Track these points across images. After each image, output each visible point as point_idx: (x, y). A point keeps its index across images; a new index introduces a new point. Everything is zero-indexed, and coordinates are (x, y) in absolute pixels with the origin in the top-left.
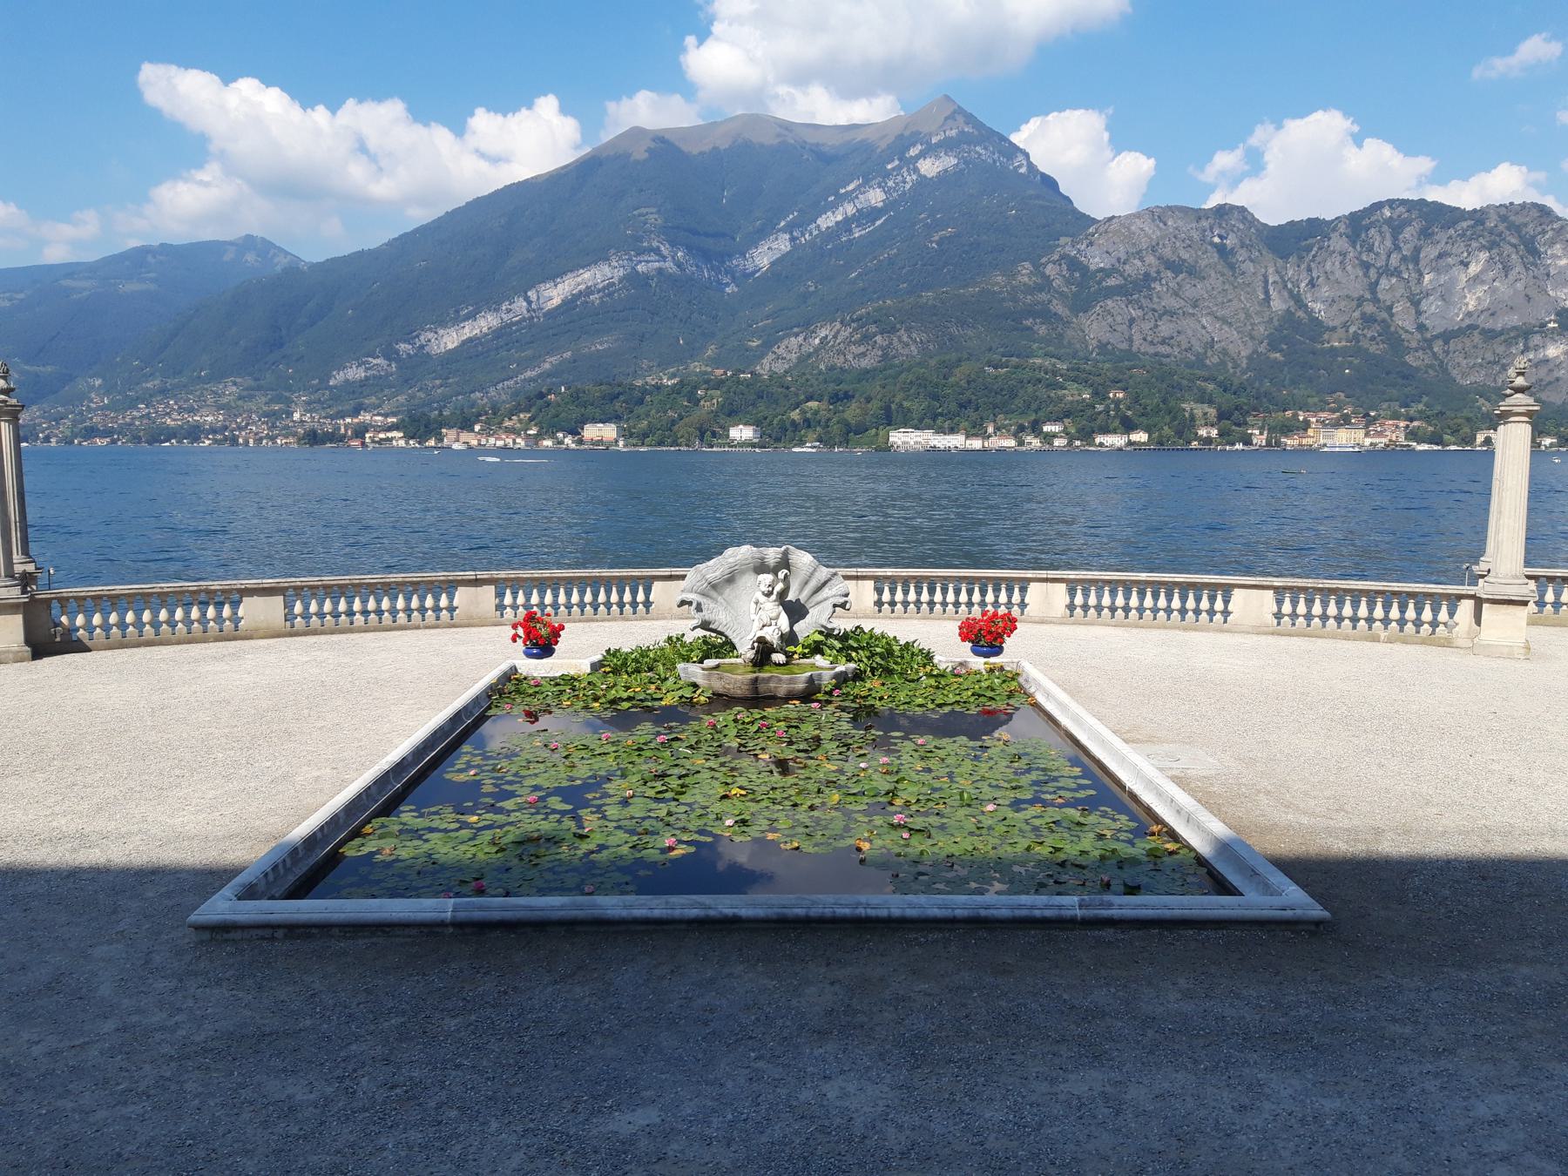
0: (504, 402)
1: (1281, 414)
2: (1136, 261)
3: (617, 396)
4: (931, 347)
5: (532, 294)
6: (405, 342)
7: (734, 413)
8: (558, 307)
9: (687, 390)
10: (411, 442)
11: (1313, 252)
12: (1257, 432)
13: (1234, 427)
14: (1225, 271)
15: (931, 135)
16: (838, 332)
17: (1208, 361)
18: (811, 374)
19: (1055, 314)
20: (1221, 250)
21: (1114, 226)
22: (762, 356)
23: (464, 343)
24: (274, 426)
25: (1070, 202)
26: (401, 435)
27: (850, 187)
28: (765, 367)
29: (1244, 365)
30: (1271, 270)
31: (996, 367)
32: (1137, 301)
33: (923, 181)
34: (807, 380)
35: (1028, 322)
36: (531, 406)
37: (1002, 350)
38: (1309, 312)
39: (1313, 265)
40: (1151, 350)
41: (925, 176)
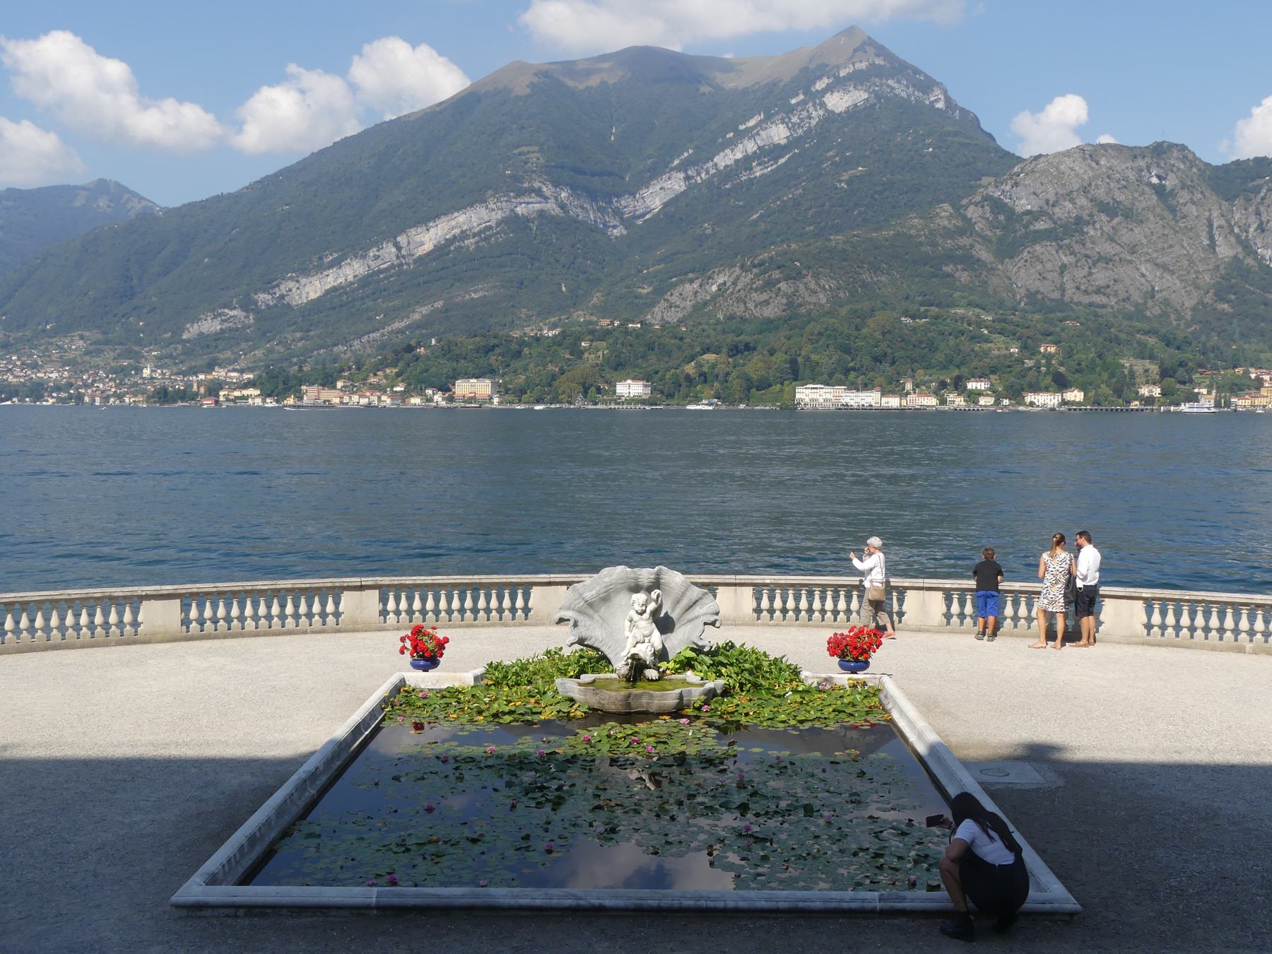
0: (369, 356)
1: (1230, 371)
2: (1067, 203)
3: (494, 347)
4: (842, 295)
5: (402, 239)
6: (264, 291)
7: (621, 366)
8: (429, 254)
9: (569, 341)
10: (268, 400)
11: (1262, 194)
12: (1204, 391)
13: (1178, 386)
14: (1166, 214)
15: (838, 67)
16: (738, 278)
17: (1148, 313)
18: (708, 324)
19: (979, 260)
20: (1159, 191)
21: (1042, 165)
22: (653, 304)
23: (327, 292)
24: (121, 384)
25: (993, 139)
26: (258, 392)
27: (752, 123)
28: (658, 316)
29: (1188, 317)
30: (1215, 214)
31: (913, 317)
32: (1069, 247)
33: (831, 117)
34: (703, 330)
35: (948, 269)
36: (398, 361)
37: (920, 298)
38: (1260, 260)
39: (1262, 209)
40: (1086, 300)
41: (833, 112)
